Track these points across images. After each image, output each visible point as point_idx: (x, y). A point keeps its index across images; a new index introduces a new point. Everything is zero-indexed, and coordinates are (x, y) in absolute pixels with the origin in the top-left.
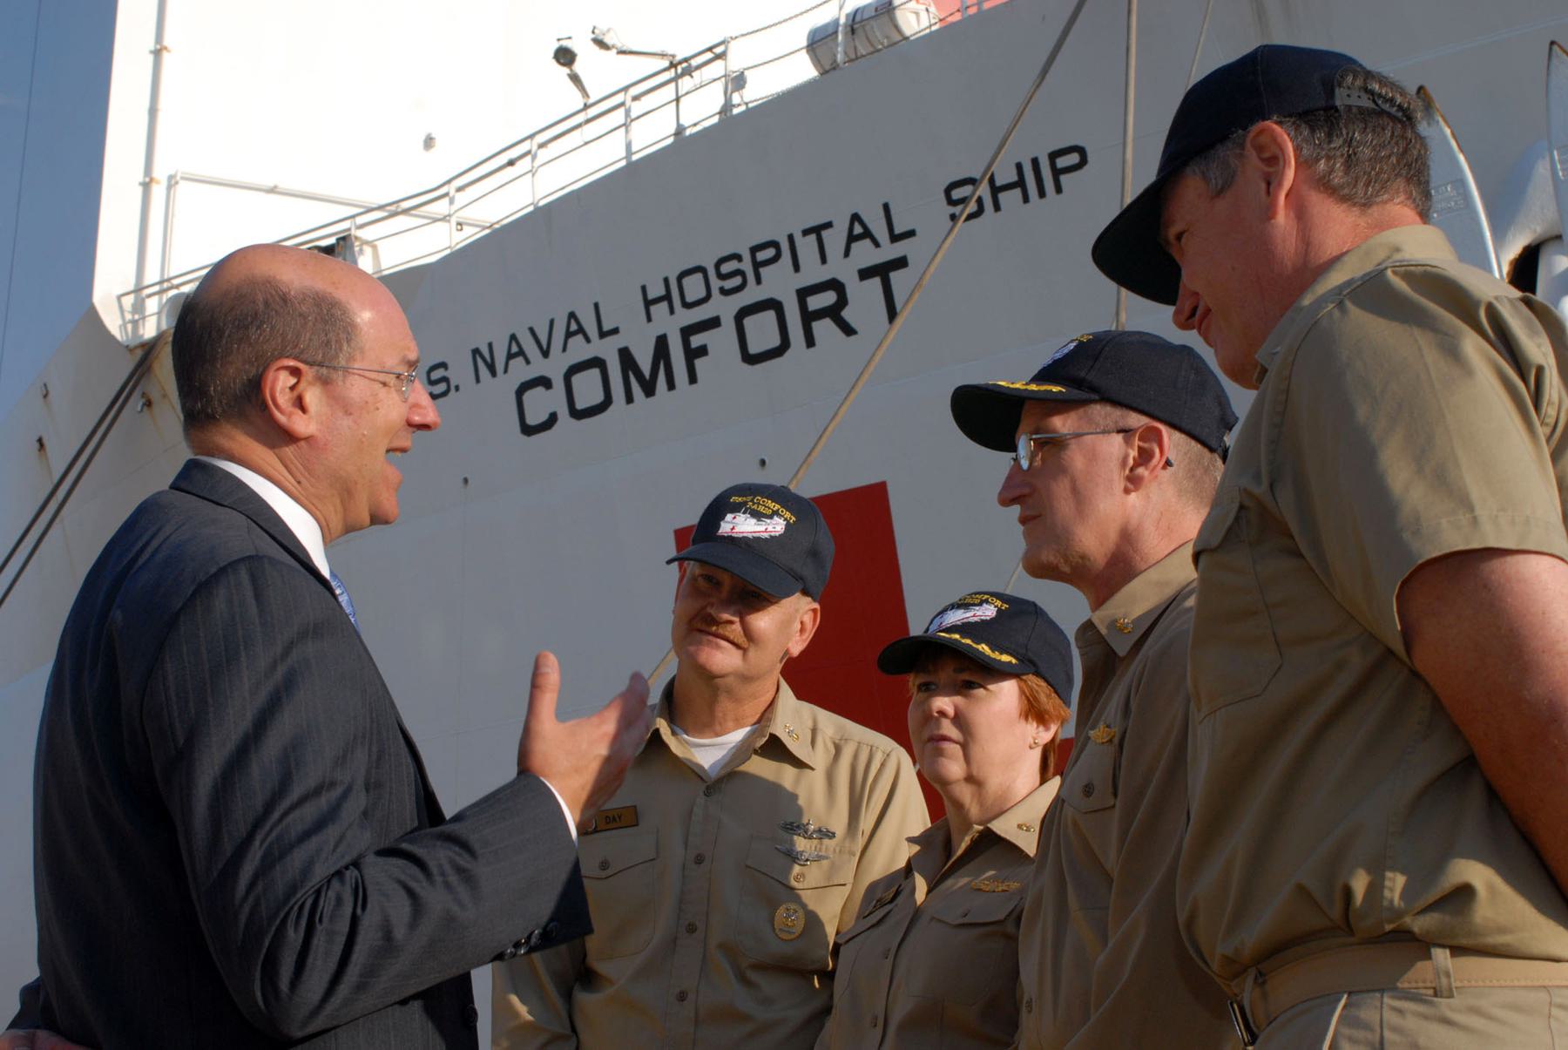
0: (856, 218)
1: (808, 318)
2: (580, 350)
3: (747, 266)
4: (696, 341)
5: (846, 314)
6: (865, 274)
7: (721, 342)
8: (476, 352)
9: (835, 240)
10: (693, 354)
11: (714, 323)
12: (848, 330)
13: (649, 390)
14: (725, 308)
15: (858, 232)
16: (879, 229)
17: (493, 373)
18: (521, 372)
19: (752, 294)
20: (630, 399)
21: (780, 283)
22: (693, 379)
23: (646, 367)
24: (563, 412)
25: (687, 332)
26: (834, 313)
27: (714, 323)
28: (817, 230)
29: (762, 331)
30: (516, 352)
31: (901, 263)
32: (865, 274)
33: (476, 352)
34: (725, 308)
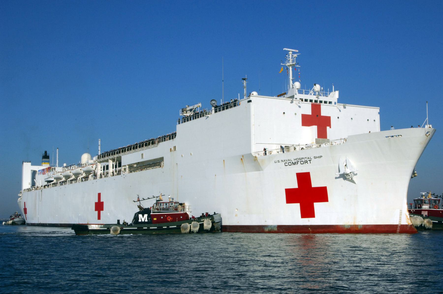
0: (308, 157)
1: (305, 162)
2: (289, 161)
3: (301, 159)
4: (298, 162)
5: (307, 162)
6: (309, 160)
7: (299, 163)
8: (282, 160)
9: (307, 158)
10: (297, 163)
11: (299, 162)
12: (308, 163)
13: (294, 164)
14: (300, 161)
15: (308, 158)
16: (310, 158)
17: (283, 161)
18: (285, 162)
19: (301, 160)
20: (293, 165)
21: (303, 160)
22: (297, 164)
23: (294, 163)
24: (288, 165)
25: (297, 162)
26: (307, 162)
27: (299, 162)
28: (306, 158)
29: (302, 163)
30: (284, 161)
31: (311, 160)
32: (309, 160)
33: (282, 160)
34: (300, 161)
